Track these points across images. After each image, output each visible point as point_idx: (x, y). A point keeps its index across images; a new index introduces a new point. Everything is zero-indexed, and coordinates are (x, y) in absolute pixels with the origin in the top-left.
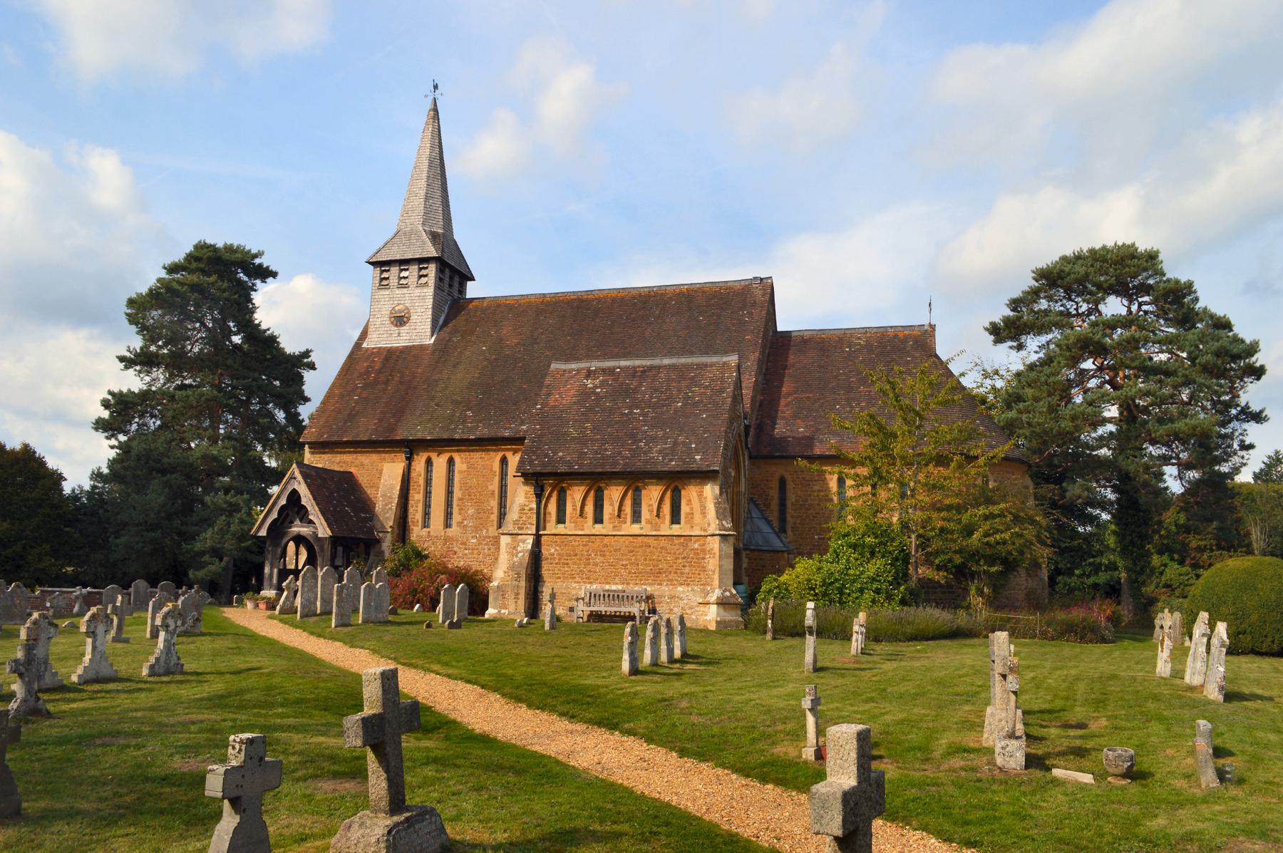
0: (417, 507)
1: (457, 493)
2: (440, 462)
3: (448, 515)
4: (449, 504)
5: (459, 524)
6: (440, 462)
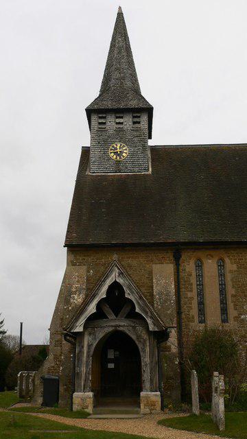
0: (191, 304)
1: (230, 291)
2: (210, 266)
3: (224, 311)
4: (223, 302)
5: (236, 318)
6: (210, 266)
